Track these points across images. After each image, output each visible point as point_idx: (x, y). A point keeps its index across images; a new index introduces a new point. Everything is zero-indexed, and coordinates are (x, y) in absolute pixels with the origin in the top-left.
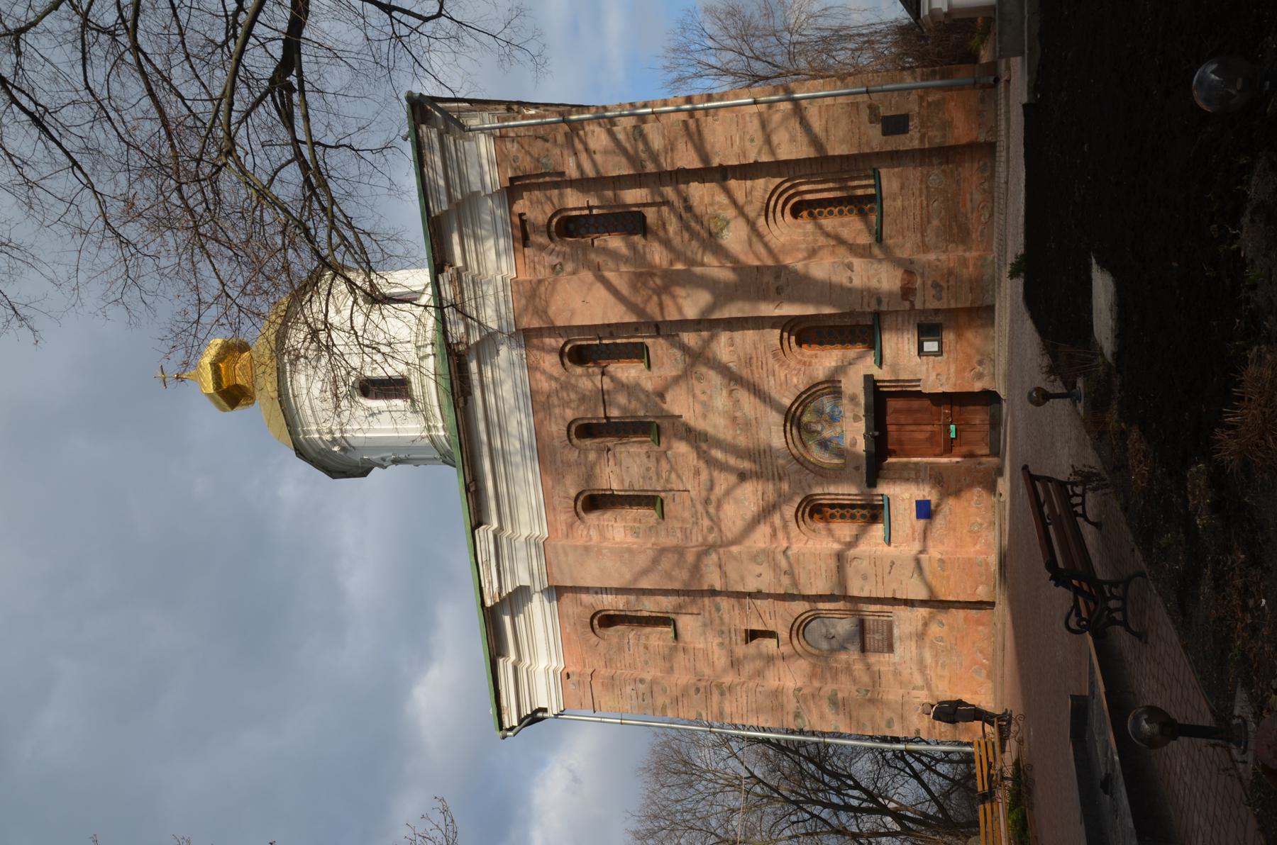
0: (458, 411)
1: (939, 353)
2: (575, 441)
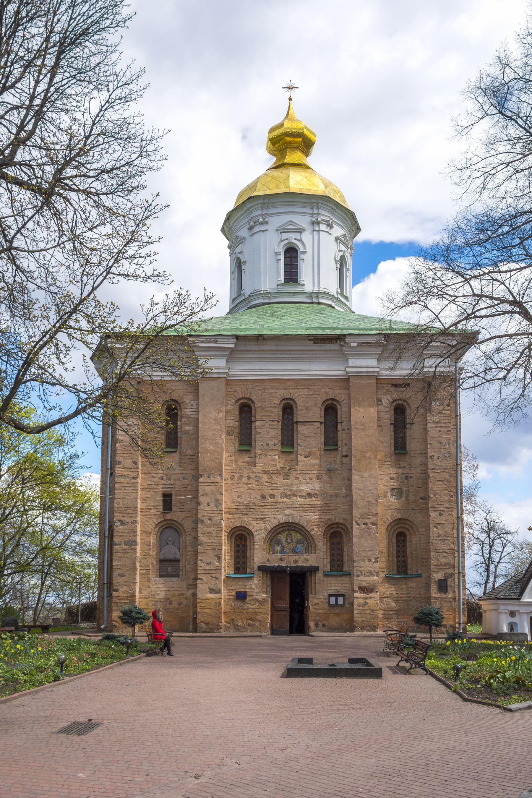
1: (330, 606)
2: (283, 402)
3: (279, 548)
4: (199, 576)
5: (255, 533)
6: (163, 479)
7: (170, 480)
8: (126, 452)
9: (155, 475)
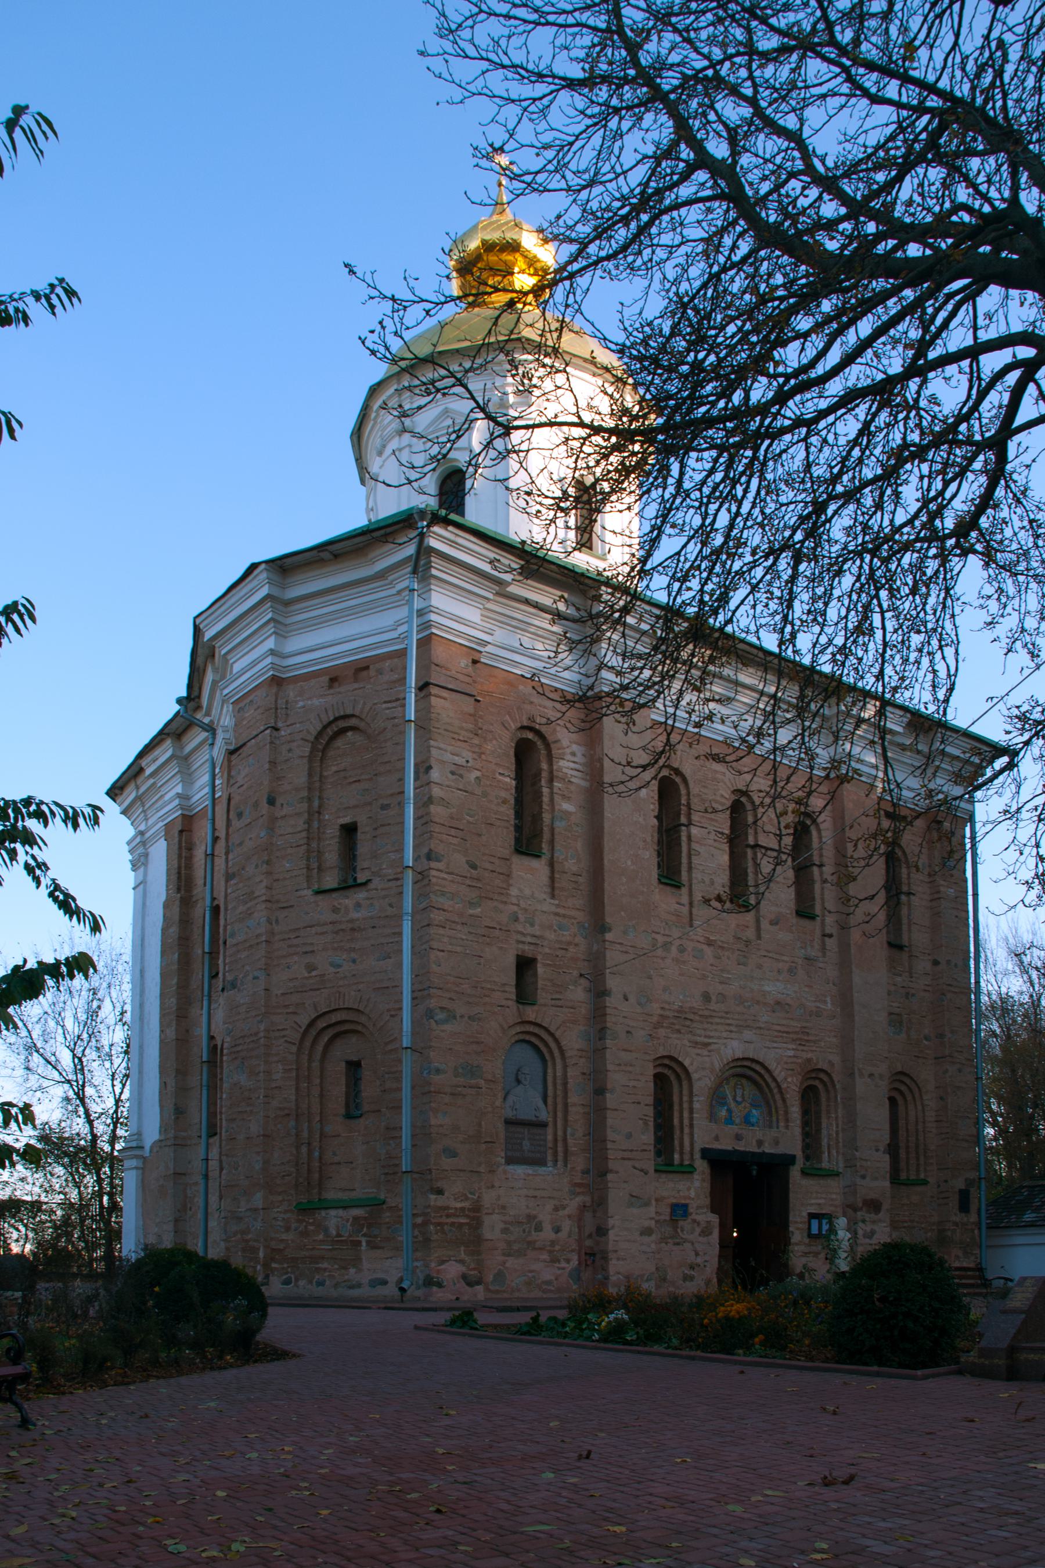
0: (315, 552)
3: (723, 1113)
4: (611, 1165)
5: (695, 1076)
6: (517, 920)
7: (532, 925)
8: (453, 832)
9: (501, 906)
